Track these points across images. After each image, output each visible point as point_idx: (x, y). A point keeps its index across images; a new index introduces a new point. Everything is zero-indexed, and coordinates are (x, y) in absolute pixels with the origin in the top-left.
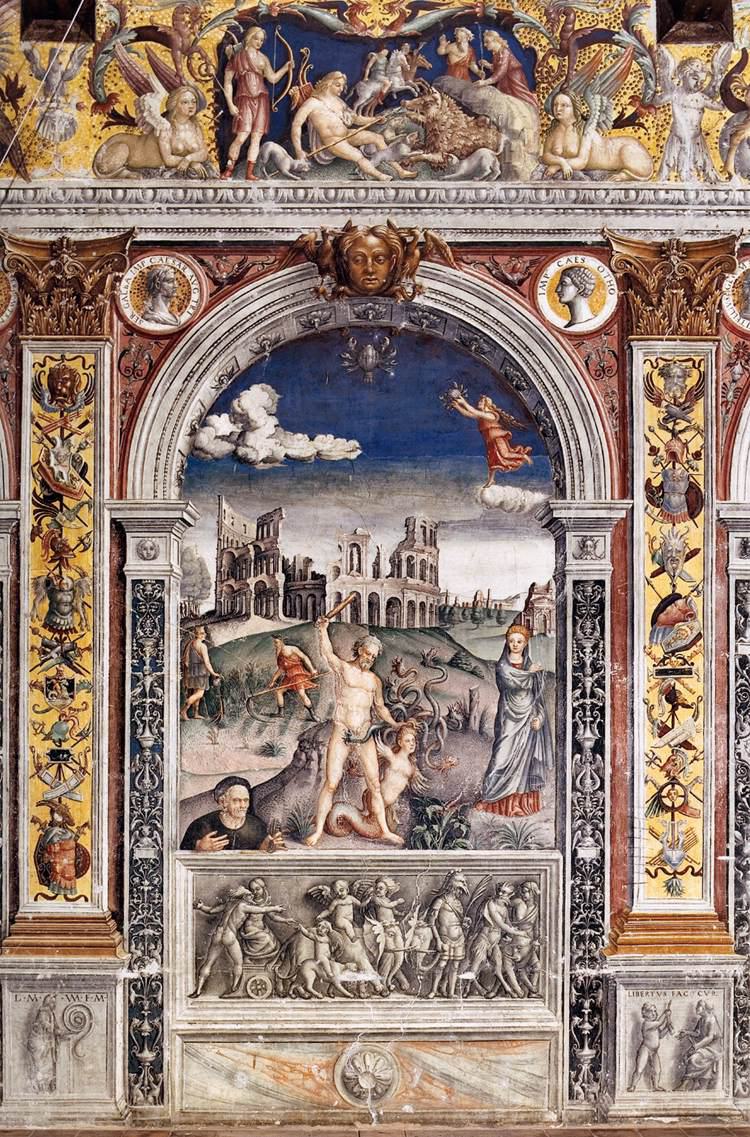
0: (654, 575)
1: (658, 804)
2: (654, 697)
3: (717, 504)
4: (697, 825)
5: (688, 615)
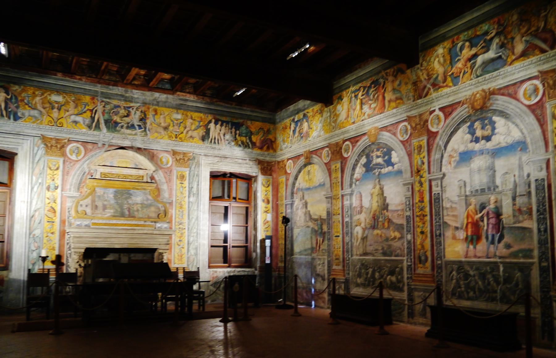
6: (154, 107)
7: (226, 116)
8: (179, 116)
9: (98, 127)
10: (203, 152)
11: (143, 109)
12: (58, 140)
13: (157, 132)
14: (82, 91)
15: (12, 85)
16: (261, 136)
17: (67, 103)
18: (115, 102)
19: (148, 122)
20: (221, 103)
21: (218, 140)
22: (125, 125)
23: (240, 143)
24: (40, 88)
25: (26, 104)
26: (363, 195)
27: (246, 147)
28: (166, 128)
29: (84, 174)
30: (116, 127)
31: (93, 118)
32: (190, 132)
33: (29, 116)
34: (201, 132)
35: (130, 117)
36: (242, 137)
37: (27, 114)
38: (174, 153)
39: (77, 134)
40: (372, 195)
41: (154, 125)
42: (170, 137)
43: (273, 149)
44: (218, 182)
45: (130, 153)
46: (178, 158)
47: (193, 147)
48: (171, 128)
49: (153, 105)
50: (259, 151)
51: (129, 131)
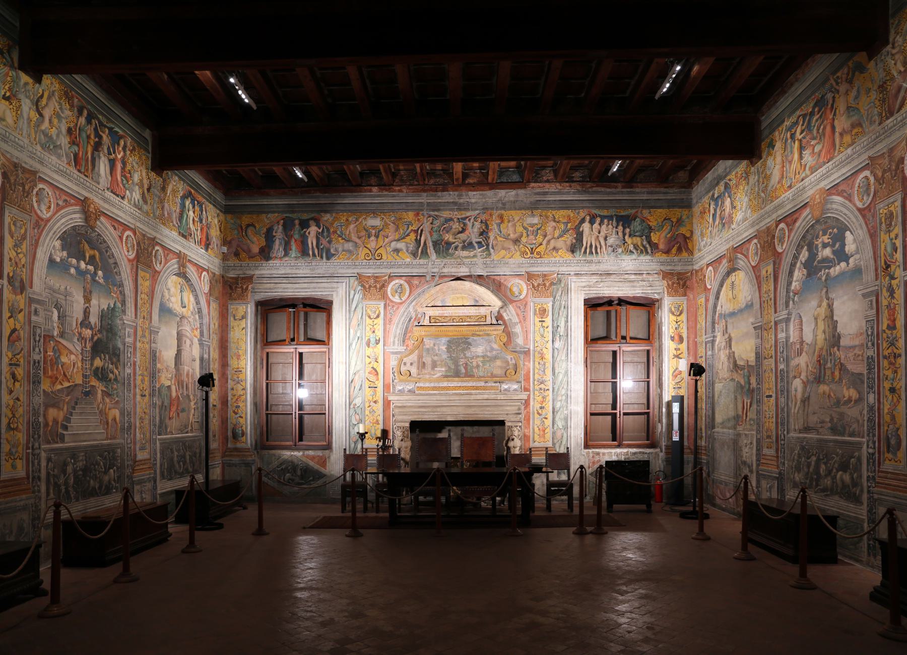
0: (9, 318)
1: (9, 428)
2: (9, 376)
3: (29, 290)
4: (20, 435)
5: (19, 339)
6: (499, 212)
7: (607, 208)
8: (535, 220)
9: (425, 254)
10: (573, 269)
11: (484, 217)
12: (376, 278)
13: (504, 248)
14: (404, 206)
15: (323, 214)
16: (667, 231)
17: (386, 225)
18: (446, 214)
19: (492, 235)
20: (599, 189)
21: (596, 247)
22: (460, 245)
23: (631, 247)
24: (353, 212)
25: (340, 236)
26: (804, 320)
27: (642, 252)
28: (517, 241)
29: (410, 320)
30: (448, 249)
31: (418, 242)
32: (552, 241)
33: (343, 251)
34: (569, 238)
35: (467, 232)
36: (634, 238)
37: (340, 249)
38: (530, 277)
39: (400, 266)
40: (816, 319)
41: (499, 239)
42: (523, 254)
43: (687, 249)
44: (600, 313)
45: (467, 284)
46: (536, 285)
47: (560, 263)
48: (524, 240)
49: (497, 209)
50: (664, 257)
51: (465, 253)
